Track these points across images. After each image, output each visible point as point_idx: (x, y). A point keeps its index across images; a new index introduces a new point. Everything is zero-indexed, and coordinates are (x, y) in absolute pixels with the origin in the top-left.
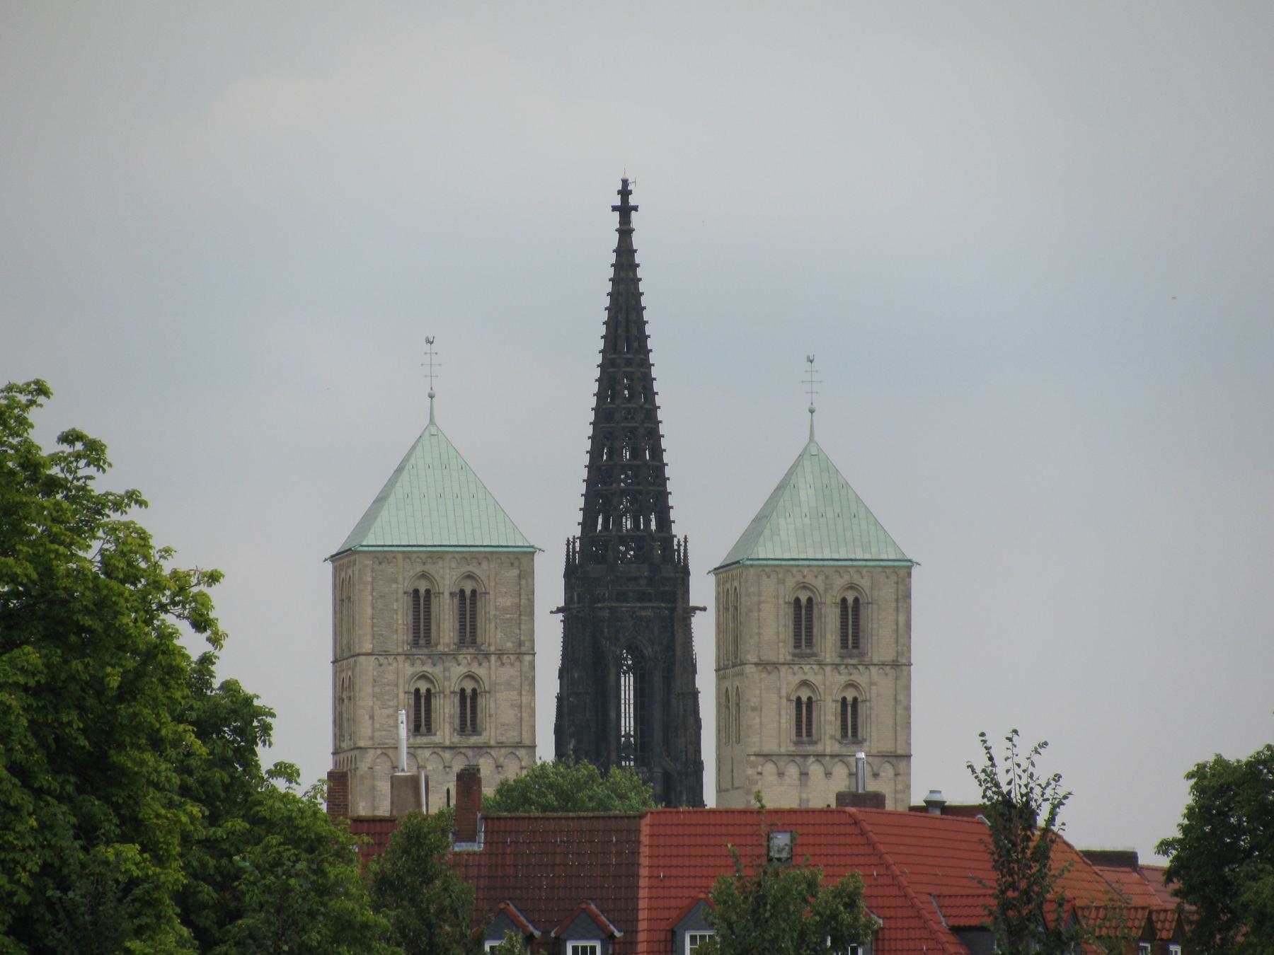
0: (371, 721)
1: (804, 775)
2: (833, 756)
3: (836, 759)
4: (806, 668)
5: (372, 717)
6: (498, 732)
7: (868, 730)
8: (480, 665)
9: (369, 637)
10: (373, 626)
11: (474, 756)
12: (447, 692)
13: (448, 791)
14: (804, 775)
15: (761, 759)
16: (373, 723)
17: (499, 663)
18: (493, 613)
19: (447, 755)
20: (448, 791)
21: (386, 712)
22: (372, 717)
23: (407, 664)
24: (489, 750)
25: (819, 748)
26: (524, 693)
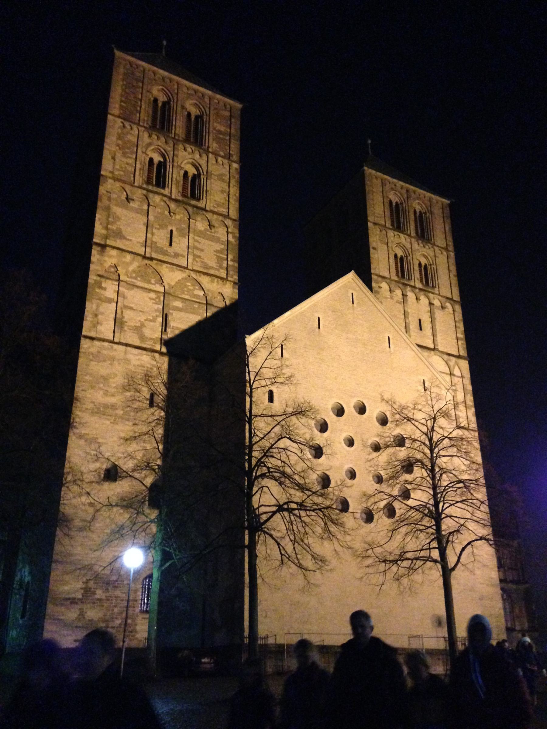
0: (113, 160)
1: (404, 295)
2: (420, 289)
3: (422, 293)
4: (401, 235)
5: (114, 158)
6: (212, 205)
7: (437, 282)
8: (200, 156)
9: (117, 106)
10: (122, 101)
11: (193, 213)
12: (175, 164)
13: (171, 231)
14: (404, 295)
15: (380, 279)
16: (114, 163)
17: (214, 162)
18: (211, 129)
19: (173, 206)
20: (171, 231)
21: (125, 160)
22: (114, 158)
23: (146, 135)
24: (204, 213)
25: (413, 284)
26: (231, 185)
